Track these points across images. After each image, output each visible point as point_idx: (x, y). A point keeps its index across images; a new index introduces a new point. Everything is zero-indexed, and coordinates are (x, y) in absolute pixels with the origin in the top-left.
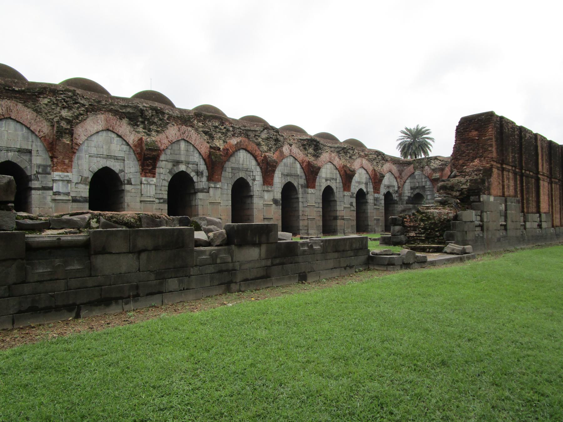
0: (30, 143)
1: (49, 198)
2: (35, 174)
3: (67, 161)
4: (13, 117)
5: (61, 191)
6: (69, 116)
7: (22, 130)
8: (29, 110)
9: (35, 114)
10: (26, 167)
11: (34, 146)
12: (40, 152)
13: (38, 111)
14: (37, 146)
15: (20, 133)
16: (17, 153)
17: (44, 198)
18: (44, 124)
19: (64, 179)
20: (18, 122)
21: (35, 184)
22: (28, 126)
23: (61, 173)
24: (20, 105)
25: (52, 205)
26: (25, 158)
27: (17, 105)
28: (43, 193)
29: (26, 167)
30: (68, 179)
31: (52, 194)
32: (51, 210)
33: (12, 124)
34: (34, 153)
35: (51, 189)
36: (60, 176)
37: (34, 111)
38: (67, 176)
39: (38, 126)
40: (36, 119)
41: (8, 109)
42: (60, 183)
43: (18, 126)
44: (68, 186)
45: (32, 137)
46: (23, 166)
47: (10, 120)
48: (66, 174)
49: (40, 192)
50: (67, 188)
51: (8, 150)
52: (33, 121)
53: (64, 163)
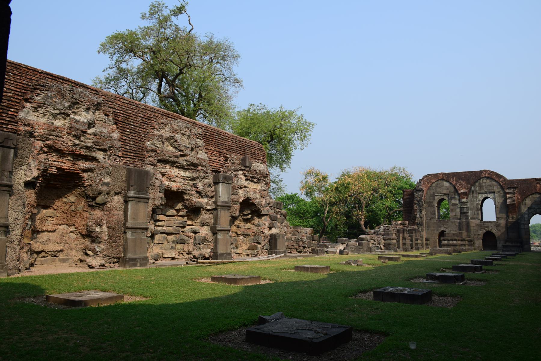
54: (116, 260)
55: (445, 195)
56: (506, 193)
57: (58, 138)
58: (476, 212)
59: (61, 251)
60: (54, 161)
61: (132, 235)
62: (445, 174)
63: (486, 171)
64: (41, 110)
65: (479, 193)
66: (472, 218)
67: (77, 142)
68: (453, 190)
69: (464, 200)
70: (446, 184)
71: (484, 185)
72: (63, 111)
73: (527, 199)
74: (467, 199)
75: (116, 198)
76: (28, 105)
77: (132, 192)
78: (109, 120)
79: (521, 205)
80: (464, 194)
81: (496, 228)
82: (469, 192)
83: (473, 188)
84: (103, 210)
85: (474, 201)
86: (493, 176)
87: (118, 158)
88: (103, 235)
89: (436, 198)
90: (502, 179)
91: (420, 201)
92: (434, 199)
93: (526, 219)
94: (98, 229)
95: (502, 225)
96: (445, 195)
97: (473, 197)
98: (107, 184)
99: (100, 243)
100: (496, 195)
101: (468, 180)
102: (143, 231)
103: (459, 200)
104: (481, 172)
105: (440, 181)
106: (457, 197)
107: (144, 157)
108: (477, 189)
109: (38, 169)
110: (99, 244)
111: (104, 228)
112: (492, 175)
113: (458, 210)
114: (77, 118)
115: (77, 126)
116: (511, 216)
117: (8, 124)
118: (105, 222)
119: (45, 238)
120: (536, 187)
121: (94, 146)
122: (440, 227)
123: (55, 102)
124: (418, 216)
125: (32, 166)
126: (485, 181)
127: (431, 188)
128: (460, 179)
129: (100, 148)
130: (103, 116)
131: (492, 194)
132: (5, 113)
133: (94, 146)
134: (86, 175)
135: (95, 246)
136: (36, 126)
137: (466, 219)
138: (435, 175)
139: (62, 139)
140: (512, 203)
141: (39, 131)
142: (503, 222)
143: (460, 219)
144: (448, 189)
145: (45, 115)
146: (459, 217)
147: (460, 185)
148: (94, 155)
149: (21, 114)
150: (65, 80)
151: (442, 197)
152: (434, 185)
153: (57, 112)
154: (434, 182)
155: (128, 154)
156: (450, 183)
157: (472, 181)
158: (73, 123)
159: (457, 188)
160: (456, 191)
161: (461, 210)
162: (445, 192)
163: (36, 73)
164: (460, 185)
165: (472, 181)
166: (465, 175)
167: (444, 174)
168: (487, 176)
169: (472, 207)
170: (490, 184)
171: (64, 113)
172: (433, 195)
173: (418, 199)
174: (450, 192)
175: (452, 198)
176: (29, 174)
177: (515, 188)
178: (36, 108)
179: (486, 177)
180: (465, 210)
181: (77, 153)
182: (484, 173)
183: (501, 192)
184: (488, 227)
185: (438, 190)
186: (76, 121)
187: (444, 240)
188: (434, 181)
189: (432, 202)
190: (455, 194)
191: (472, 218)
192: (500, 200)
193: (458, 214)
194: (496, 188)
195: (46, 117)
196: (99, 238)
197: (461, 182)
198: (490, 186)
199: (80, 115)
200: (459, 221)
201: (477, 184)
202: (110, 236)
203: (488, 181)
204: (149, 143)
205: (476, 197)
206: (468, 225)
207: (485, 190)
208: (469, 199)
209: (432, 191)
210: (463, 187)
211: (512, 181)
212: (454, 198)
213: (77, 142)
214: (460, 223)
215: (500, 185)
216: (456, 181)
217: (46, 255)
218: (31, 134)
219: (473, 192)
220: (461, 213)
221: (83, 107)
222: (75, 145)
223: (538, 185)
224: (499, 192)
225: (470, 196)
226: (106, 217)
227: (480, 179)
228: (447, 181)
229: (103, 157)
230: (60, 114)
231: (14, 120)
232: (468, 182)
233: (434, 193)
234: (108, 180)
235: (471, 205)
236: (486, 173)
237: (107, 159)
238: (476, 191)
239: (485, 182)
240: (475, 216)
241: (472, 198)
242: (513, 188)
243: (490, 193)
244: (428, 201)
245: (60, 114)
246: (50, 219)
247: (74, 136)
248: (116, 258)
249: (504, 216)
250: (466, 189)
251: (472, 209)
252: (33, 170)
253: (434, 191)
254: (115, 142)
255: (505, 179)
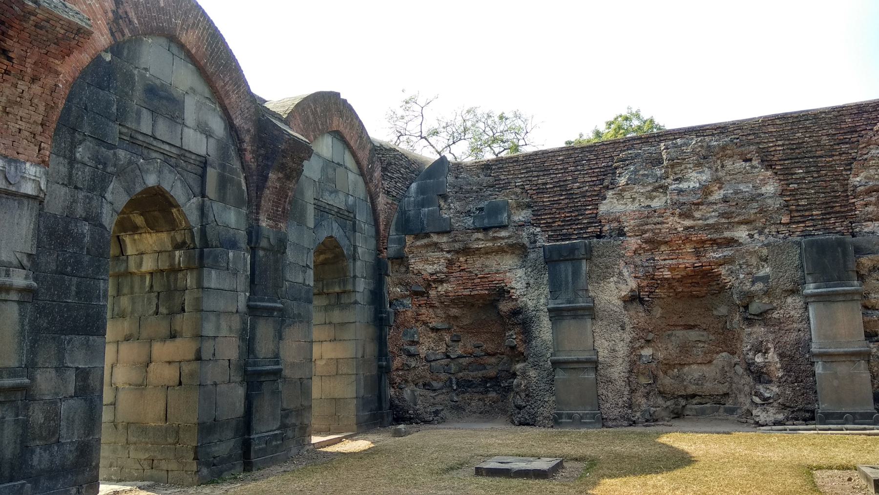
54: (807, 415)
57: (658, 226)
59: (726, 395)
60: (665, 260)
61: (824, 368)
64: (627, 195)
67: (688, 223)
72: (657, 184)
75: (789, 300)
76: (610, 194)
77: (812, 286)
78: (753, 167)
84: (766, 325)
87: (782, 228)
88: (772, 368)
94: (759, 359)
98: (765, 279)
99: (770, 382)
102: (853, 358)
107: (852, 210)
109: (635, 277)
110: (768, 386)
111: (772, 356)
114: (684, 185)
115: (683, 199)
117: (587, 228)
118: (769, 345)
119: (696, 375)
121: (723, 220)
123: (643, 175)
125: (626, 274)
129: (736, 220)
130: (740, 164)
132: (581, 215)
133: (723, 220)
134: (723, 270)
135: (761, 388)
136: (623, 218)
139: (665, 225)
141: (629, 224)
145: (634, 199)
148: (727, 234)
149: (603, 208)
150: (662, 136)
153: (650, 188)
155: (807, 213)
158: (676, 197)
163: (616, 145)
171: (661, 187)
176: (623, 287)
178: (620, 194)
181: (695, 239)
186: (680, 192)
195: (637, 201)
196: (766, 373)
199: (688, 180)
202: (787, 369)
204: (858, 179)
213: (688, 223)
217: (703, 401)
218: (621, 233)
221: (688, 166)
222: (687, 228)
226: (771, 337)
229: (747, 233)
230: (655, 189)
231: (596, 219)
234: (767, 270)
237: (756, 236)
245: (655, 189)
246: (700, 345)
247: (680, 215)
248: (808, 411)
252: (628, 280)
254: (769, 201)
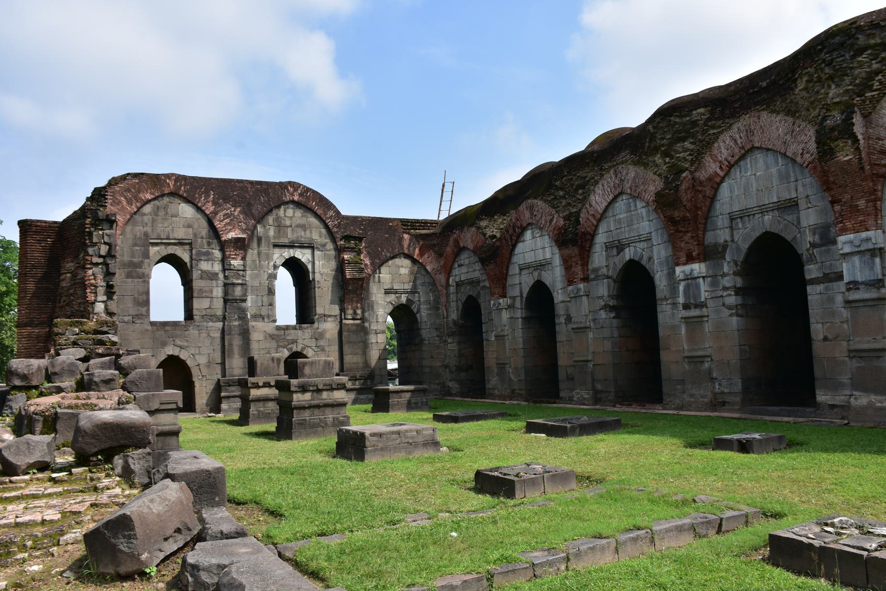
0: (792, 185)
1: (839, 299)
2: (808, 250)
3: (862, 203)
4: (757, 145)
5: (859, 278)
6: (838, 95)
7: (777, 163)
8: (780, 117)
9: (790, 120)
10: (795, 238)
11: (800, 189)
12: (812, 198)
13: (791, 112)
14: (805, 186)
15: (774, 170)
16: (776, 213)
17: (831, 300)
18: (809, 134)
19: (862, 248)
20: (768, 150)
21: (812, 271)
22: (783, 151)
23: (852, 236)
24: (764, 115)
25: (845, 313)
26: (789, 218)
27: (759, 118)
28: (826, 289)
29: (795, 238)
30: (871, 246)
31: (843, 289)
32: (845, 326)
33: (760, 157)
34: (802, 204)
35: (840, 277)
36: (851, 242)
37: (787, 115)
38: (868, 240)
39: (799, 143)
40: (793, 132)
41: (750, 132)
42: (856, 259)
43: (770, 158)
44: (873, 263)
45: (794, 172)
46: (789, 238)
47: (756, 152)
48: (864, 235)
49: (820, 288)
50: (872, 268)
51: (763, 210)
52: (788, 137)
53: (855, 209)
55: (180, 243)
56: (339, 250)
58: (265, 299)
62: (185, 178)
63: (295, 185)
65: (276, 246)
66: (255, 317)
68: (203, 228)
69: (236, 263)
70: (186, 211)
71: (288, 223)
73: (384, 269)
74: (244, 259)
79: (371, 284)
80: (241, 245)
81: (313, 343)
82: (251, 237)
83: (259, 228)
85: (261, 266)
86: (312, 203)
89: (153, 250)
90: (331, 213)
91: (110, 255)
92: (146, 255)
93: (380, 320)
95: (328, 336)
96: (180, 243)
97: (259, 254)
100: (317, 253)
101: (249, 205)
103: (223, 260)
104: (283, 186)
105: (166, 199)
106: (217, 254)
108: (271, 233)
112: (307, 198)
113: (218, 292)
116: (350, 312)
120: (401, 239)
122: (164, 344)
124: (100, 307)
126: (290, 212)
127: (137, 217)
128: (226, 200)
131: (308, 252)
137: (240, 318)
138: (155, 180)
140: (357, 276)
142: (330, 328)
143: (224, 318)
144: (189, 226)
146: (219, 313)
147: (227, 216)
151: (171, 250)
152: (147, 209)
154: (149, 201)
156: (199, 209)
157: (257, 209)
159: (217, 223)
160: (215, 232)
161: (226, 293)
162: (181, 233)
164: (227, 216)
165: (257, 209)
166: (242, 188)
167: (180, 178)
168: (296, 198)
169: (256, 283)
170: (303, 221)
172: (146, 242)
173: (104, 250)
174: (195, 235)
175: (199, 253)
177: (360, 239)
179: (293, 202)
180: (238, 291)
182: (291, 190)
183: (330, 246)
184: (294, 341)
185: (160, 228)
187: (303, 389)
188: (149, 196)
189: (140, 265)
190: (209, 244)
191: (255, 317)
192: (322, 268)
193: (219, 304)
194: (317, 234)
197: (229, 209)
198: (303, 227)
200: (220, 325)
201: (270, 219)
203: (299, 213)
205: (269, 257)
206: (245, 334)
207: (291, 235)
208: (249, 258)
209: (139, 230)
210: (233, 223)
211: (355, 220)
212: (207, 254)
214: (223, 331)
215: (326, 226)
216: (215, 203)
219: (259, 240)
220: (226, 301)
223: (406, 236)
224: (324, 245)
225: (252, 254)
227: (278, 207)
228: (187, 201)
232: (247, 212)
233: (146, 234)
235: (253, 277)
236: (295, 190)
238: (268, 237)
239: (290, 214)
240: (264, 312)
241: (255, 257)
242: (355, 238)
243: (302, 247)
244: (126, 258)
249: (335, 310)
250: (243, 231)
251: (255, 289)
253: (148, 229)
255: (338, 213)
